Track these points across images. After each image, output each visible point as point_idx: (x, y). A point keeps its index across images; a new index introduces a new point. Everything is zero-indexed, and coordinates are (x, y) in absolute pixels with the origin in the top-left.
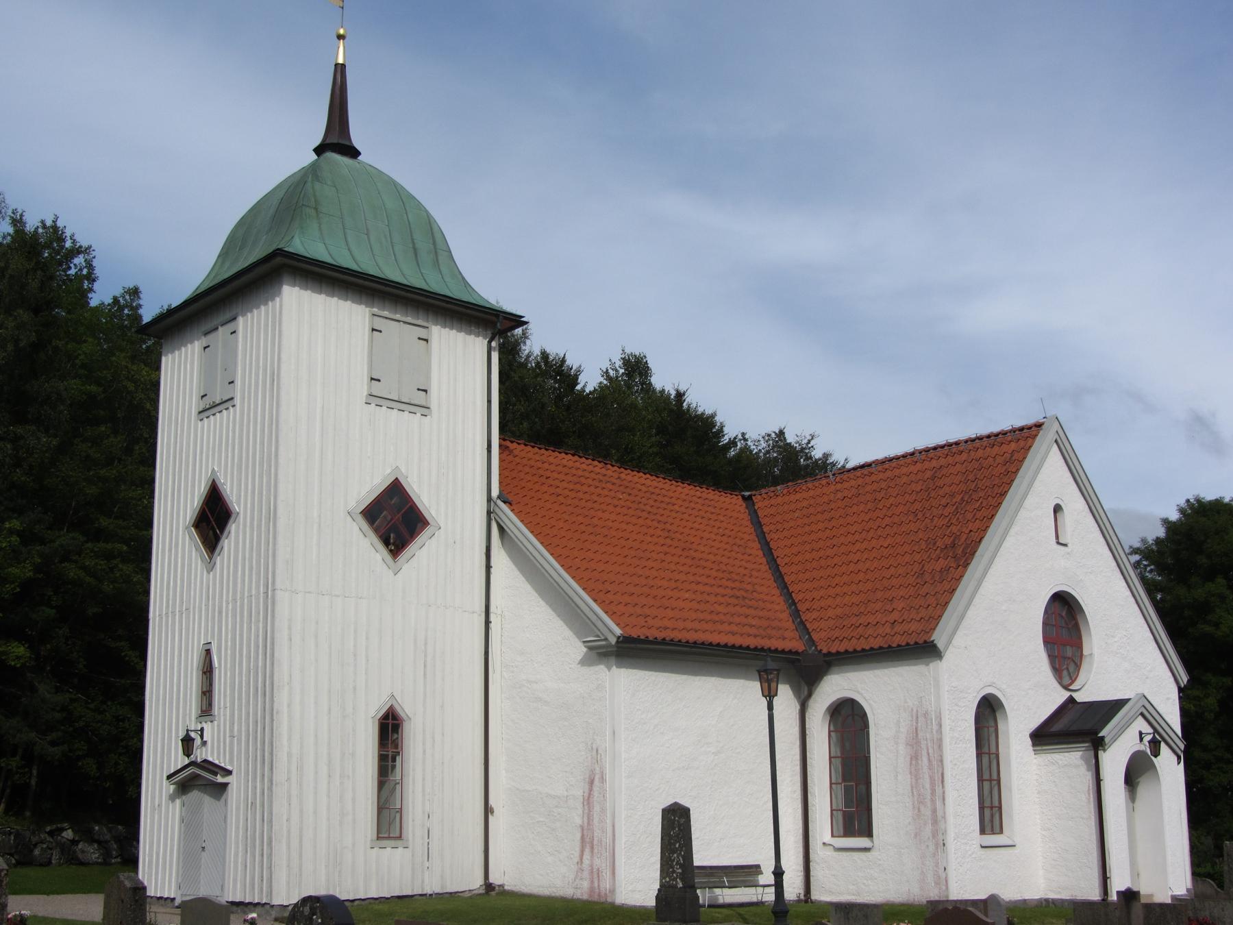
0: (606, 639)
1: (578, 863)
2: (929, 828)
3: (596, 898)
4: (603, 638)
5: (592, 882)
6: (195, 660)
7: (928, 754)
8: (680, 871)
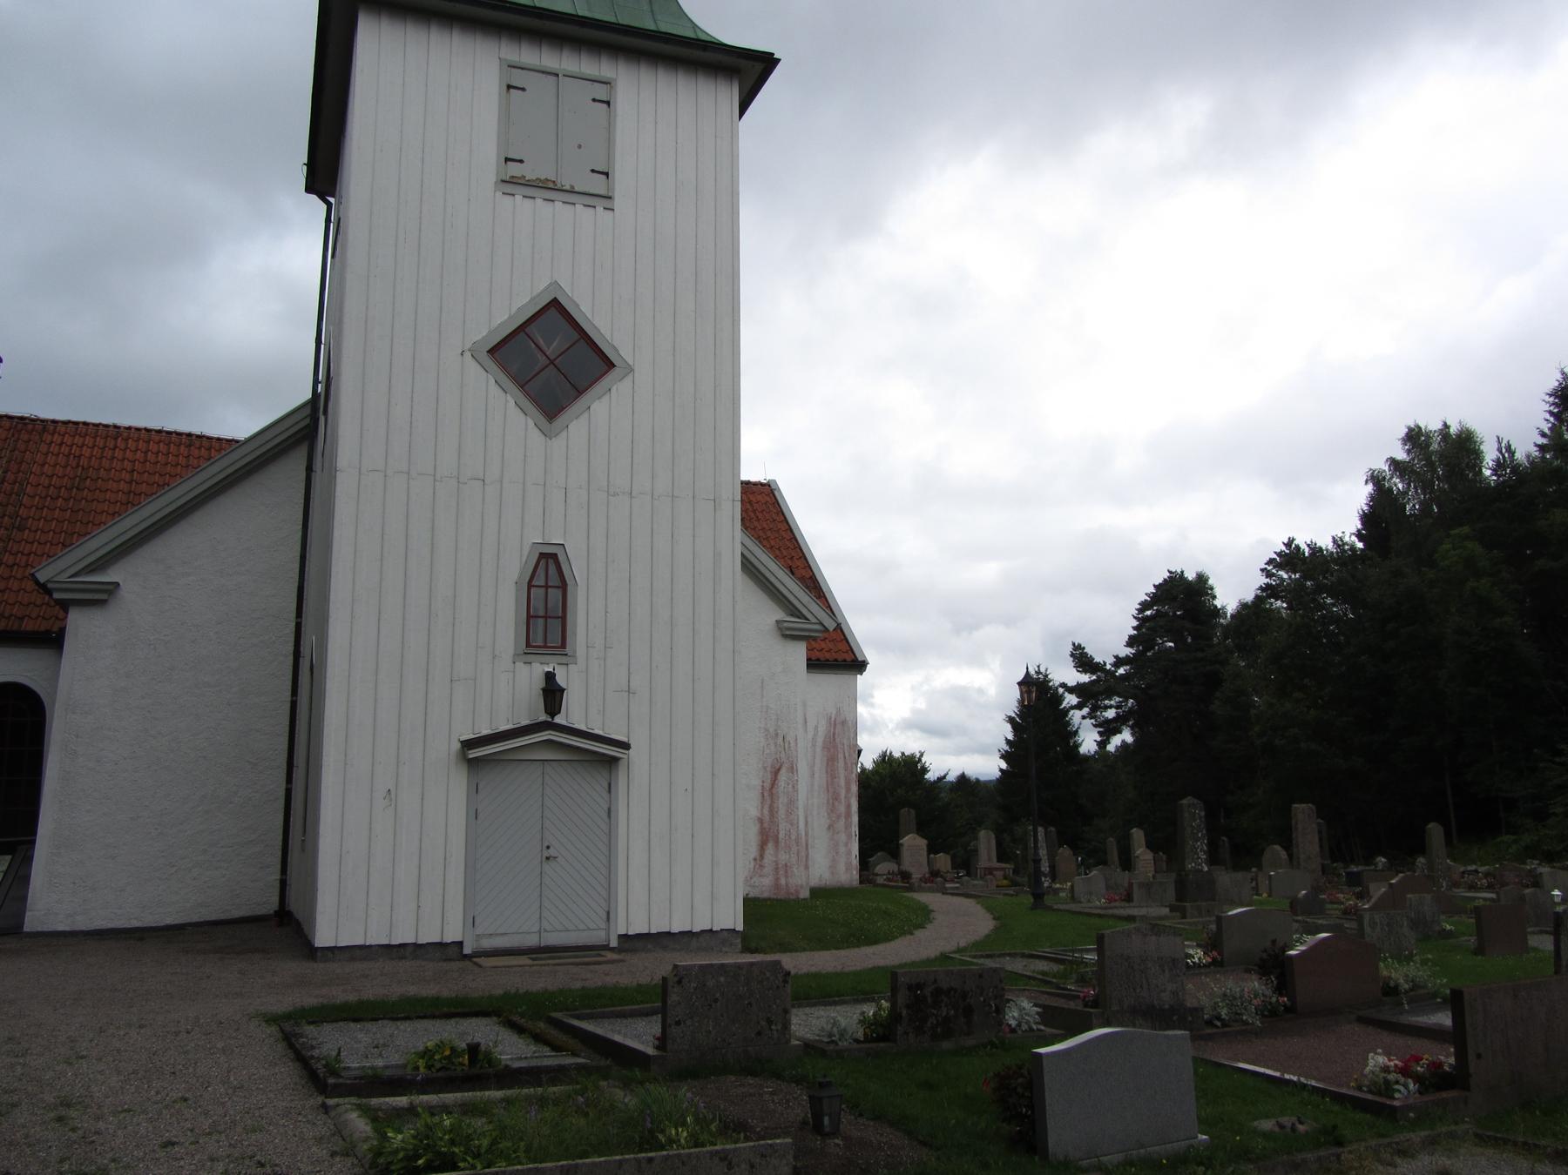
0: (821, 624)
1: (755, 859)
2: (842, 822)
3: (782, 895)
5: (777, 879)
6: (515, 566)
7: (845, 757)
8: (1204, 857)
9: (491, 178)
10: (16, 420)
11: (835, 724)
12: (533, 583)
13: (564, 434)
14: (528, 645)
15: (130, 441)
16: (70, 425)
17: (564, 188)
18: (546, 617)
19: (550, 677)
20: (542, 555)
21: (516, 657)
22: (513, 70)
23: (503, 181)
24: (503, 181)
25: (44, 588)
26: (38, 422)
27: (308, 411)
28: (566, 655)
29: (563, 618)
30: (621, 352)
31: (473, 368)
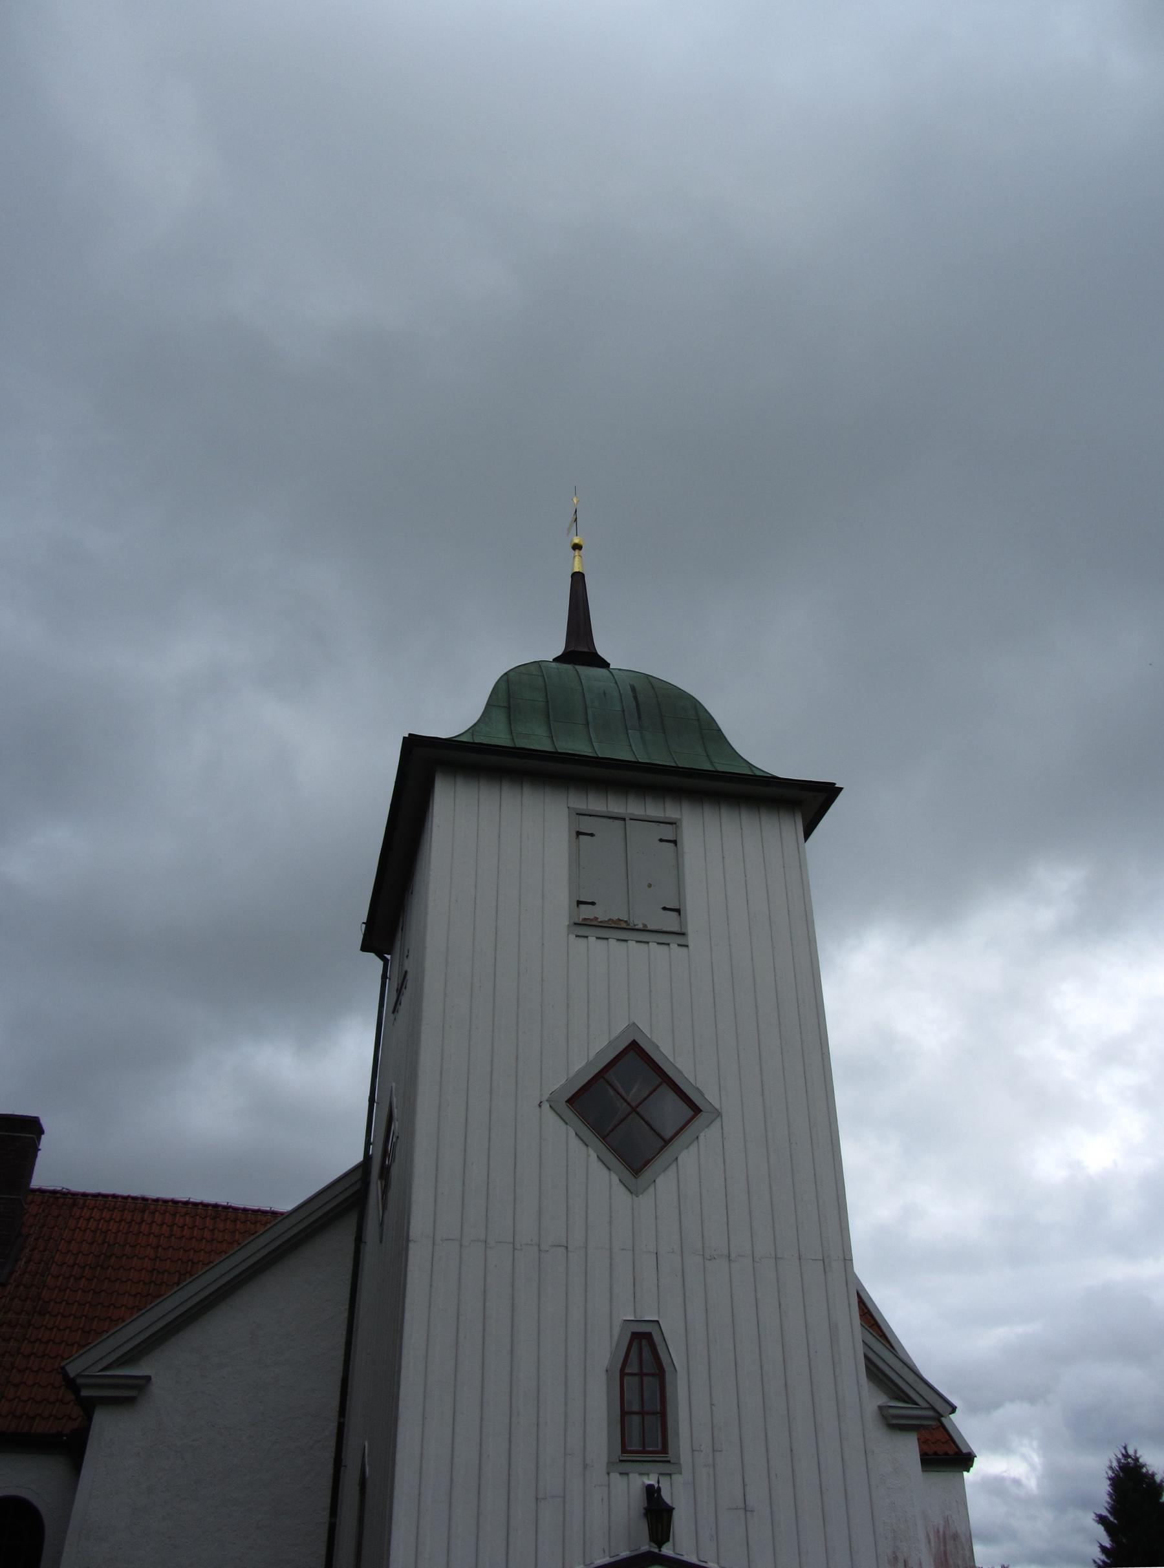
0: (933, 1409)
4: (927, 1406)
9: (565, 922)
10: (48, 1194)
11: (945, 1539)
12: (627, 1370)
13: (651, 1190)
14: (624, 1450)
15: (157, 1214)
16: (100, 1198)
17: (636, 927)
18: (642, 1413)
19: (652, 1493)
20: (636, 1336)
21: (611, 1467)
22: (581, 817)
23: (576, 924)
24: (576, 924)
25: (72, 1384)
26: (69, 1196)
27: (358, 1175)
28: (669, 1462)
29: (662, 1415)
30: (706, 1096)
31: (550, 1118)
